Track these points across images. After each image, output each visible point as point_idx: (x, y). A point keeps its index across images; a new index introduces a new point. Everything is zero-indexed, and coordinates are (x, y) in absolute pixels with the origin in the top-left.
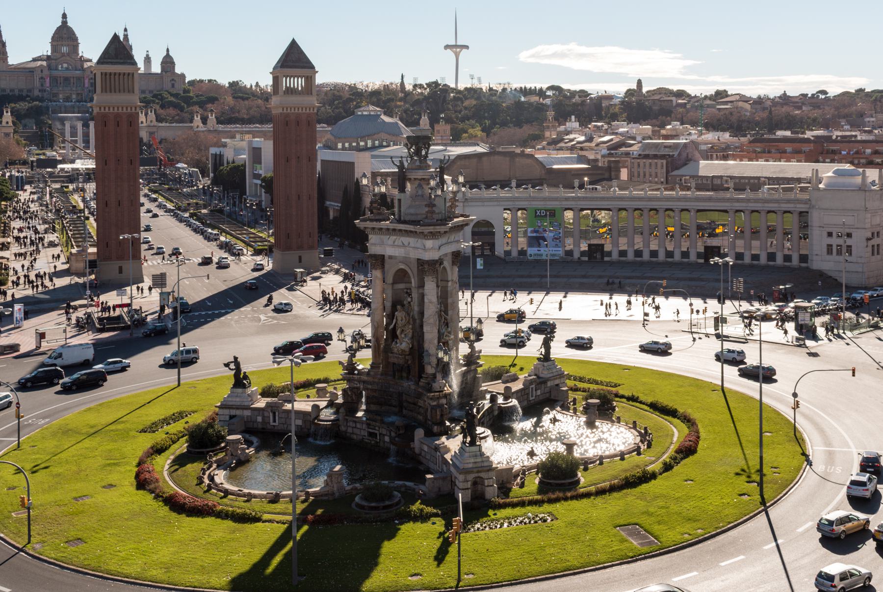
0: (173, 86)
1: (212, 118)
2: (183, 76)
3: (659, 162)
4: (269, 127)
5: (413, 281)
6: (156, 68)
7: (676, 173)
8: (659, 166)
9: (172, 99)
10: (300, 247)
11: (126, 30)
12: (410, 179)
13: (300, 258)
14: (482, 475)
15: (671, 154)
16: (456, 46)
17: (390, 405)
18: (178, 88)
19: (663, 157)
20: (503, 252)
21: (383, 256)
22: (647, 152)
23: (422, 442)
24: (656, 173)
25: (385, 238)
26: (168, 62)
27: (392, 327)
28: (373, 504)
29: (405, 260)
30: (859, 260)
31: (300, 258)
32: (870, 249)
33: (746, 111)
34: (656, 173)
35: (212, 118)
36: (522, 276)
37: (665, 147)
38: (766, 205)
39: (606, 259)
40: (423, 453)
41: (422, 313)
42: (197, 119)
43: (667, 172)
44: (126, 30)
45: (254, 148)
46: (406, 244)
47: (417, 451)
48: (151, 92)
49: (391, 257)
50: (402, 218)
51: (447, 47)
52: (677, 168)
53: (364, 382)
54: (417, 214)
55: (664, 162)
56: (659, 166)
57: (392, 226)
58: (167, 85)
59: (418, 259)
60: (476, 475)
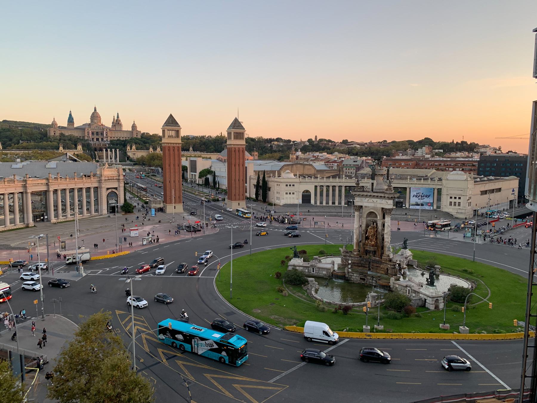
0: (137, 136)
2: (140, 132)
5: (378, 217)
10: (239, 200)
11: (118, 114)
13: (239, 203)
14: (439, 298)
18: (139, 137)
23: (394, 283)
25: (363, 199)
26: (134, 127)
27: (367, 235)
29: (374, 208)
31: (239, 203)
32: (468, 203)
36: (321, 212)
41: (383, 230)
42: (151, 149)
44: (118, 114)
45: (191, 160)
46: (375, 201)
47: (391, 287)
48: (129, 138)
49: (366, 207)
50: (374, 191)
54: (379, 189)
57: (369, 194)
58: (135, 136)
59: (383, 208)
60: (436, 298)
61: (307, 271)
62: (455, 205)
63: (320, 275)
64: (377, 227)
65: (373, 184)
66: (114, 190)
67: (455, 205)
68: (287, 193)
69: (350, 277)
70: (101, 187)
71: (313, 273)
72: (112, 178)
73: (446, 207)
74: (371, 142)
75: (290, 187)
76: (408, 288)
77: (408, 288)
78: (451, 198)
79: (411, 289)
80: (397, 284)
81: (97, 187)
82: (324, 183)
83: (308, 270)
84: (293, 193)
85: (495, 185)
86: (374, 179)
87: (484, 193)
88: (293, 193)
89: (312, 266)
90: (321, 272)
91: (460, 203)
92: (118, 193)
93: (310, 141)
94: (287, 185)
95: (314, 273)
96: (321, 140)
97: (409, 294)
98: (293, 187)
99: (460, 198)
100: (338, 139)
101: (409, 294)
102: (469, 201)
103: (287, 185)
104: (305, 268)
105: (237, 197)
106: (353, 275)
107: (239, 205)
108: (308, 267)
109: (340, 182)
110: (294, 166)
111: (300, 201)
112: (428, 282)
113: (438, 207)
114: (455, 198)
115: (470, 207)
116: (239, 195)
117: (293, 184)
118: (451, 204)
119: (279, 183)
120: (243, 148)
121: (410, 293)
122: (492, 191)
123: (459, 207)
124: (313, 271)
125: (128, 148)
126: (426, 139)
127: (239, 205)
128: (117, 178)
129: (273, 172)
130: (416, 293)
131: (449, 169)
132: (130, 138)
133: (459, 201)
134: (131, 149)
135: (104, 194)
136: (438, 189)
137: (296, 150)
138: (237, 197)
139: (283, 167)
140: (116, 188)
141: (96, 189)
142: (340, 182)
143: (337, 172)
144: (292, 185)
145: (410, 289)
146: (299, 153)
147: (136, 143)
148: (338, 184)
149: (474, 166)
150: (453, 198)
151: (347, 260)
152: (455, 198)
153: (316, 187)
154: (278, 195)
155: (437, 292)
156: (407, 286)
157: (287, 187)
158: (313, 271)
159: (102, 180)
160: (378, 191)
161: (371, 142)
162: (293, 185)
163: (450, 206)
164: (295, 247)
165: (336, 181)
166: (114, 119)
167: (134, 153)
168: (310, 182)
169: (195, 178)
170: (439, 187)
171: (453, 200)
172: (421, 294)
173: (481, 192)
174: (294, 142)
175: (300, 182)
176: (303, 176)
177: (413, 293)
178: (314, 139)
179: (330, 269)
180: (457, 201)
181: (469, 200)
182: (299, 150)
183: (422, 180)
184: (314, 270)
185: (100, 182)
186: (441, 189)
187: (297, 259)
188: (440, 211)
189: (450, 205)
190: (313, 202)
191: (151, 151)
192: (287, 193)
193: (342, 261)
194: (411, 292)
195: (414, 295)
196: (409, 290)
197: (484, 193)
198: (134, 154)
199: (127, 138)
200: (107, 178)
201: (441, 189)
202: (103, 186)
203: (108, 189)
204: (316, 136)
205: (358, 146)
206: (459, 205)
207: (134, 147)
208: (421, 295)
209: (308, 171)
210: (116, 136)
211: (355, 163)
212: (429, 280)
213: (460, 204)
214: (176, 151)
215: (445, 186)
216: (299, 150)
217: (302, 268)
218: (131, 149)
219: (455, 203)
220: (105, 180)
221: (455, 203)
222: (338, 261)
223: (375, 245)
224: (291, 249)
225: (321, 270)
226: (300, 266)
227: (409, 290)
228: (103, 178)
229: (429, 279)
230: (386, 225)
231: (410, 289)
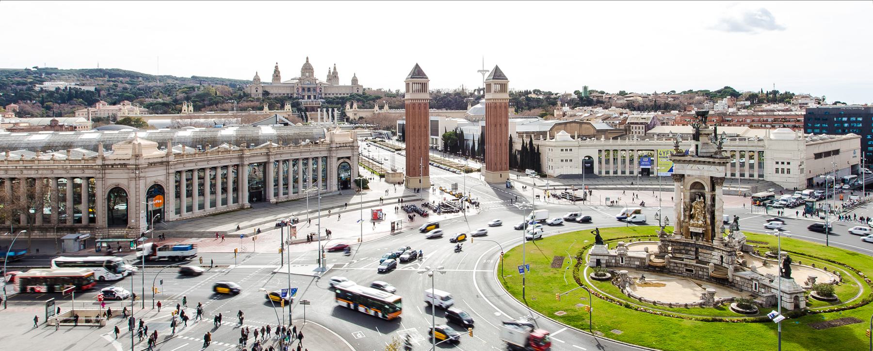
0: (358, 91)
1: (386, 107)
3: (641, 126)
4: (403, 111)
6: (349, 83)
7: (649, 132)
8: (641, 128)
9: (359, 97)
12: (701, 134)
15: (647, 122)
16: (483, 71)
17: (689, 254)
18: (361, 92)
19: (642, 124)
20: (598, 172)
21: (684, 175)
22: (632, 121)
23: (733, 275)
24: (639, 132)
26: (355, 80)
28: (748, 311)
30: (795, 176)
33: (641, 101)
34: (639, 132)
35: (386, 107)
37: (642, 119)
38: (739, 148)
39: (651, 175)
40: (735, 282)
42: (376, 108)
43: (646, 131)
47: (730, 280)
48: (347, 94)
51: (479, 71)
52: (650, 129)
53: (672, 242)
55: (644, 126)
56: (641, 128)
58: (355, 92)
61: (613, 261)
62: (783, 172)
63: (632, 266)
64: (704, 202)
65: (697, 146)
66: (347, 160)
67: (783, 172)
68: (562, 161)
69: (672, 268)
70: (331, 157)
71: (622, 264)
72: (345, 145)
73: (770, 176)
74: (655, 93)
75: (567, 152)
76: (754, 282)
77: (754, 282)
78: (777, 163)
79: (759, 283)
80: (738, 276)
81: (326, 157)
82: (610, 147)
83: (616, 260)
84: (571, 160)
85: (831, 145)
86: (699, 141)
87: (818, 156)
88: (571, 160)
89: (620, 255)
90: (631, 263)
91: (789, 169)
92: (351, 164)
93: (576, 92)
94: (562, 150)
95: (624, 264)
96: (591, 92)
97: (756, 289)
98: (571, 152)
99: (789, 163)
100: (612, 89)
101: (756, 289)
102: (801, 167)
103: (562, 150)
104: (611, 258)
105: (499, 166)
106: (677, 266)
107: (501, 177)
108: (616, 256)
109: (631, 145)
110: (568, 125)
111: (579, 171)
112: (782, 272)
113: (761, 176)
114: (783, 163)
115: (803, 175)
116: (501, 164)
117: (571, 148)
118: (777, 171)
119: (552, 148)
120: (505, 103)
121: (757, 287)
122: (828, 154)
123: (788, 175)
124: (622, 262)
125: (348, 106)
126: (726, 88)
127: (501, 177)
128: (351, 144)
129: (544, 134)
130: (766, 288)
131: (765, 126)
132: (349, 95)
133: (788, 167)
134: (351, 107)
135: (334, 164)
136: (759, 151)
137: (562, 105)
138: (498, 166)
139: (554, 127)
140: (349, 158)
141: (325, 159)
142: (631, 145)
143: (623, 132)
144: (569, 150)
145: (757, 283)
146: (566, 108)
147: (358, 100)
148: (629, 147)
149: (798, 121)
150: (780, 163)
151: (666, 246)
152: (783, 163)
153: (600, 151)
154: (550, 164)
155: (795, 287)
156: (752, 279)
157: (562, 152)
158: (622, 262)
159: (332, 148)
160: (705, 155)
161: (655, 93)
162: (571, 150)
163: (777, 174)
164: (597, 229)
165: (625, 143)
166: (330, 72)
167: (355, 113)
168: (592, 146)
169: (437, 144)
170: (761, 149)
171: (780, 166)
172: (774, 288)
173: (815, 154)
174: (556, 94)
175: (580, 146)
176: (583, 137)
177: (761, 288)
178: (581, 90)
179: (644, 259)
180: (786, 167)
181: (801, 165)
182: (566, 104)
183: (737, 140)
184: (624, 260)
185: (330, 151)
186: (763, 152)
187: (600, 246)
188: (763, 180)
189: (776, 172)
190: (596, 171)
191: (377, 111)
192: (562, 161)
193: (660, 247)
194: (759, 287)
195: (763, 290)
196: (756, 284)
197: (818, 156)
198: (355, 114)
199: (346, 95)
200: (338, 146)
201: (763, 152)
202: (334, 155)
203: (339, 159)
204: (585, 88)
205: (640, 99)
206: (789, 171)
207: (355, 105)
208: (773, 290)
209: (585, 130)
210: (333, 93)
211: (643, 121)
212: (784, 271)
213: (789, 171)
214: (422, 108)
215: (768, 148)
216: (566, 104)
217: (607, 258)
218: (351, 107)
219: (783, 169)
220: (336, 147)
221: (783, 169)
222: (654, 248)
223: (703, 225)
224: (592, 232)
225: (632, 259)
226: (605, 256)
227: (756, 284)
228: (334, 145)
229: (784, 268)
230: (717, 198)
231: (757, 283)
